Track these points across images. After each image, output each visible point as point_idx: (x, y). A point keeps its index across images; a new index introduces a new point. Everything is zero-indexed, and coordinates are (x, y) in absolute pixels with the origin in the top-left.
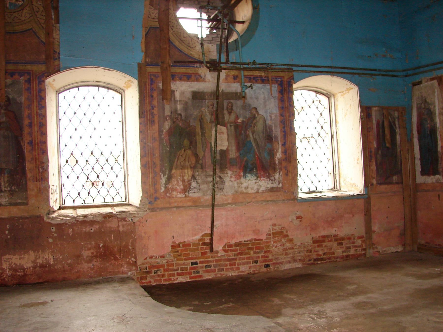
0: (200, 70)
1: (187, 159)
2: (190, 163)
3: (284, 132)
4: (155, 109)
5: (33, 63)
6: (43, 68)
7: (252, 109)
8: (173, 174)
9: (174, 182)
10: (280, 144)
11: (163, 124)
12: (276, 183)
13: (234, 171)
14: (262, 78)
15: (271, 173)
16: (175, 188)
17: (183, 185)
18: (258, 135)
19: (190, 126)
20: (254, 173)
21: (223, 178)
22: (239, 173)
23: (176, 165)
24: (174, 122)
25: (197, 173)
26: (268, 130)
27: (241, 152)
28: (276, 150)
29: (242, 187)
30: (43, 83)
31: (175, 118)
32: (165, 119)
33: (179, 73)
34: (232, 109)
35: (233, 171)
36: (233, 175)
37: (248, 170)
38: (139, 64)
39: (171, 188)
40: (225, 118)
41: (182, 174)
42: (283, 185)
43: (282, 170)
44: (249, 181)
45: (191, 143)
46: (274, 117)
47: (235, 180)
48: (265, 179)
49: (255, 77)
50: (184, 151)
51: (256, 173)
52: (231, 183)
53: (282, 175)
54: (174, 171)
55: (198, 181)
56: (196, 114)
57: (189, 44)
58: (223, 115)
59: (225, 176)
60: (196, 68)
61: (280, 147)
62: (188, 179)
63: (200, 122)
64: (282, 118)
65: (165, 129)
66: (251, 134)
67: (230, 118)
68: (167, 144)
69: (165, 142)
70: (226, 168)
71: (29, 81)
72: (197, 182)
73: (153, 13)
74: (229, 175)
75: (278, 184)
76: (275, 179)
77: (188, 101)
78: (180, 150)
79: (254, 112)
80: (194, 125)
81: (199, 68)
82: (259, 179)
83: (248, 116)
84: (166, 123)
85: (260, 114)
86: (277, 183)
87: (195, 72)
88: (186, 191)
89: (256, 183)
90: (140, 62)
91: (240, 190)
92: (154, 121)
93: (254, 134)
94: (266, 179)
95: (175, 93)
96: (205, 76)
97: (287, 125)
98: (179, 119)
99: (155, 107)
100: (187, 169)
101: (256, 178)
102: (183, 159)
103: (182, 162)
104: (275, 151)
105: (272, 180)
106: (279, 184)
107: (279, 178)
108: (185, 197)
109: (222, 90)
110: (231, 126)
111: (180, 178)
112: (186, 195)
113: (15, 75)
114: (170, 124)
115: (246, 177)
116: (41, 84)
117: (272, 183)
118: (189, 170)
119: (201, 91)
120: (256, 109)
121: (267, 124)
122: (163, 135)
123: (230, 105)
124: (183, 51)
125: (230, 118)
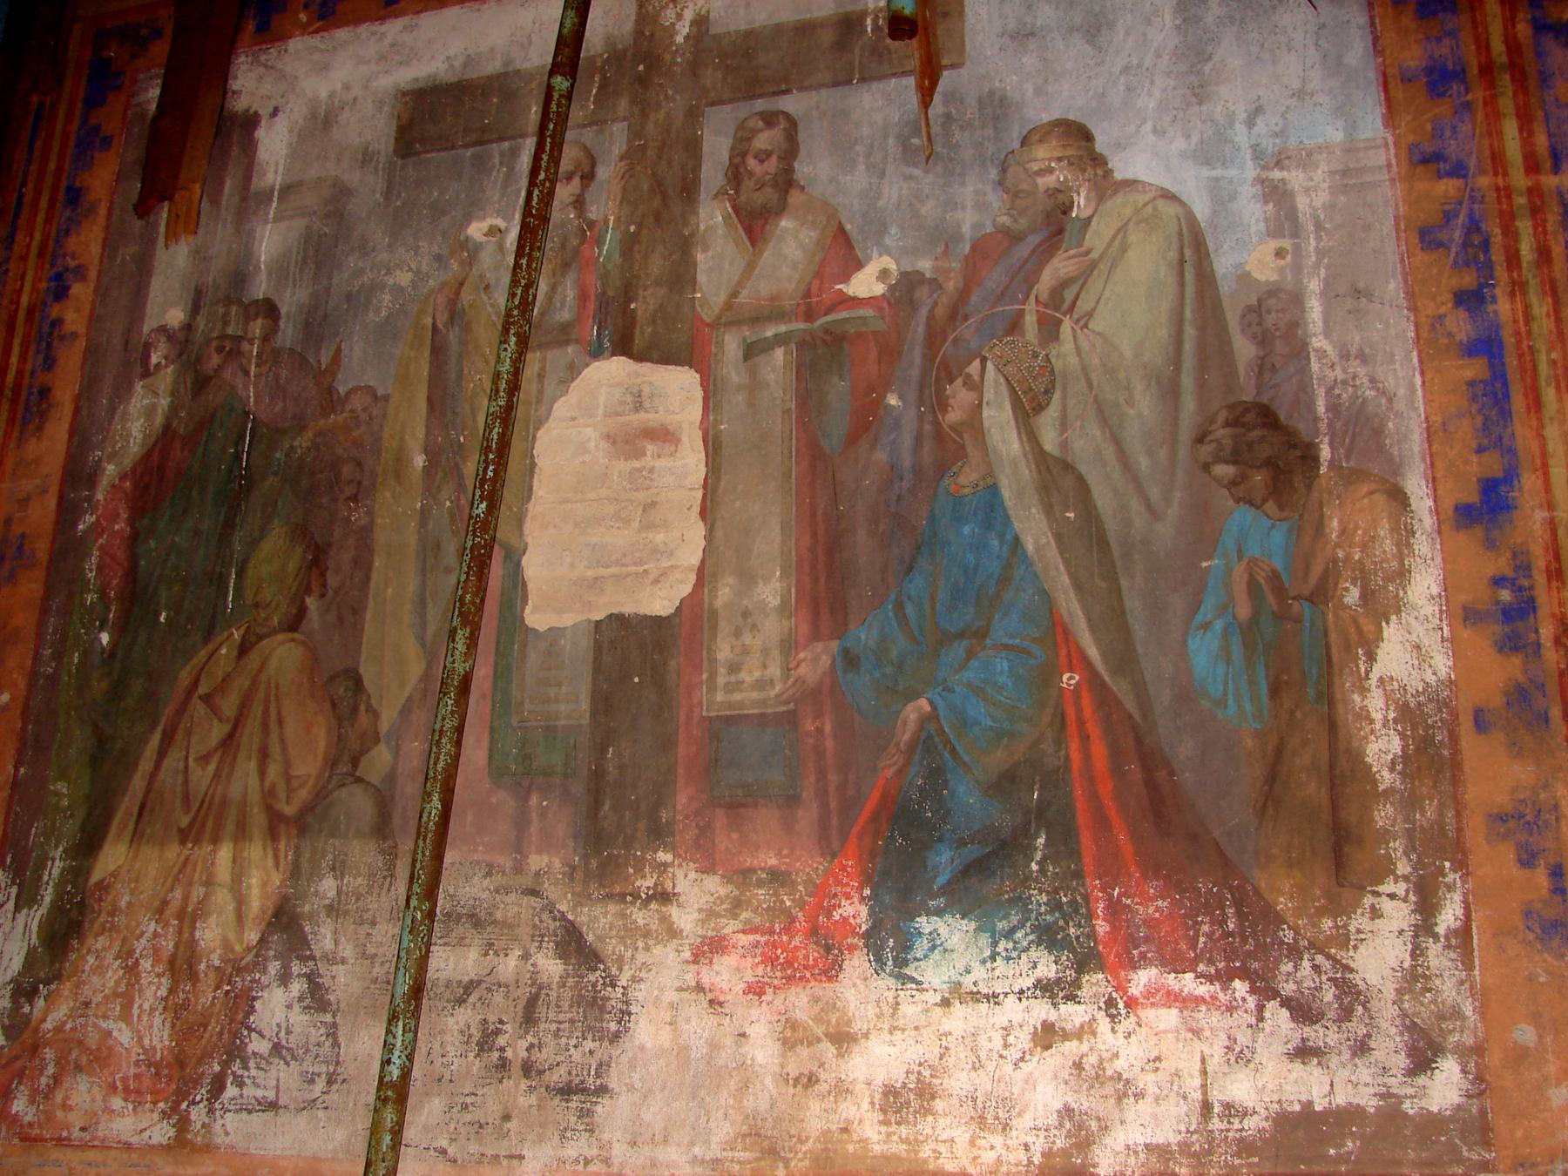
1: (250, 733)
2: (274, 771)
3: (1486, 346)
4: (77, 289)
7: (1025, 142)
8: (102, 887)
9: (99, 970)
10: (1416, 486)
11: (112, 410)
12: (1361, 1048)
13: (747, 872)
15: (1283, 904)
16: (93, 1040)
17: (176, 1009)
18: (1104, 421)
19: (330, 401)
20: (1020, 902)
21: (611, 947)
22: (822, 899)
23: (148, 791)
24: (201, 383)
25: (328, 886)
26: (1244, 350)
27: (863, 635)
28: (1367, 596)
29: (842, 1090)
31: (220, 349)
32: (137, 365)
34: (786, 182)
35: (742, 876)
36: (730, 927)
37: (944, 861)
39: (59, 1029)
40: (702, 278)
41: (178, 894)
42: (1480, 1083)
43: (1461, 865)
44: (946, 1003)
45: (317, 560)
46: (1321, 198)
47: (756, 990)
48: (1188, 983)
50: (243, 650)
51: (1056, 906)
52: (698, 1026)
53: (1463, 934)
54: (113, 857)
55: (322, 967)
56: (404, 278)
58: (684, 248)
59: (631, 932)
61: (1423, 545)
62: (227, 945)
63: (438, 351)
64: (1448, 187)
65: (112, 457)
66: (999, 419)
67: (750, 266)
68: (103, 594)
69: (91, 575)
70: (659, 834)
72: (312, 979)
74: (685, 919)
75: (1402, 1061)
76: (1351, 996)
77: (353, 178)
78: (207, 639)
79: (1050, 171)
80: (371, 391)
82: (1095, 983)
83: (968, 222)
84: (139, 399)
85: (1131, 184)
86: (1390, 1049)
88: (197, 1082)
89: (1047, 1036)
91: (816, 1118)
92: (45, 393)
93: (1039, 408)
94: (1203, 990)
95: (260, 133)
97: (1513, 260)
98: (245, 346)
99: (80, 273)
100: (242, 833)
101: (1047, 968)
102: (218, 732)
103: (205, 759)
104: (1352, 596)
105: (1302, 1011)
106: (1422, 1060)
107: (1414, 978)
108: (167, 1148)
109: (701, 22)
110: (751, 352)
111: (156, 935)
112: (183, 1124)
114: (164, 402)
115: (905, 946)
117: (1304, 1052)
118: (255, 851)
119: (493, 67)
120: (1077, 134)
121: (1225, 287)
122: (93, 510)
123: (763, 140)
125: (750, 266)
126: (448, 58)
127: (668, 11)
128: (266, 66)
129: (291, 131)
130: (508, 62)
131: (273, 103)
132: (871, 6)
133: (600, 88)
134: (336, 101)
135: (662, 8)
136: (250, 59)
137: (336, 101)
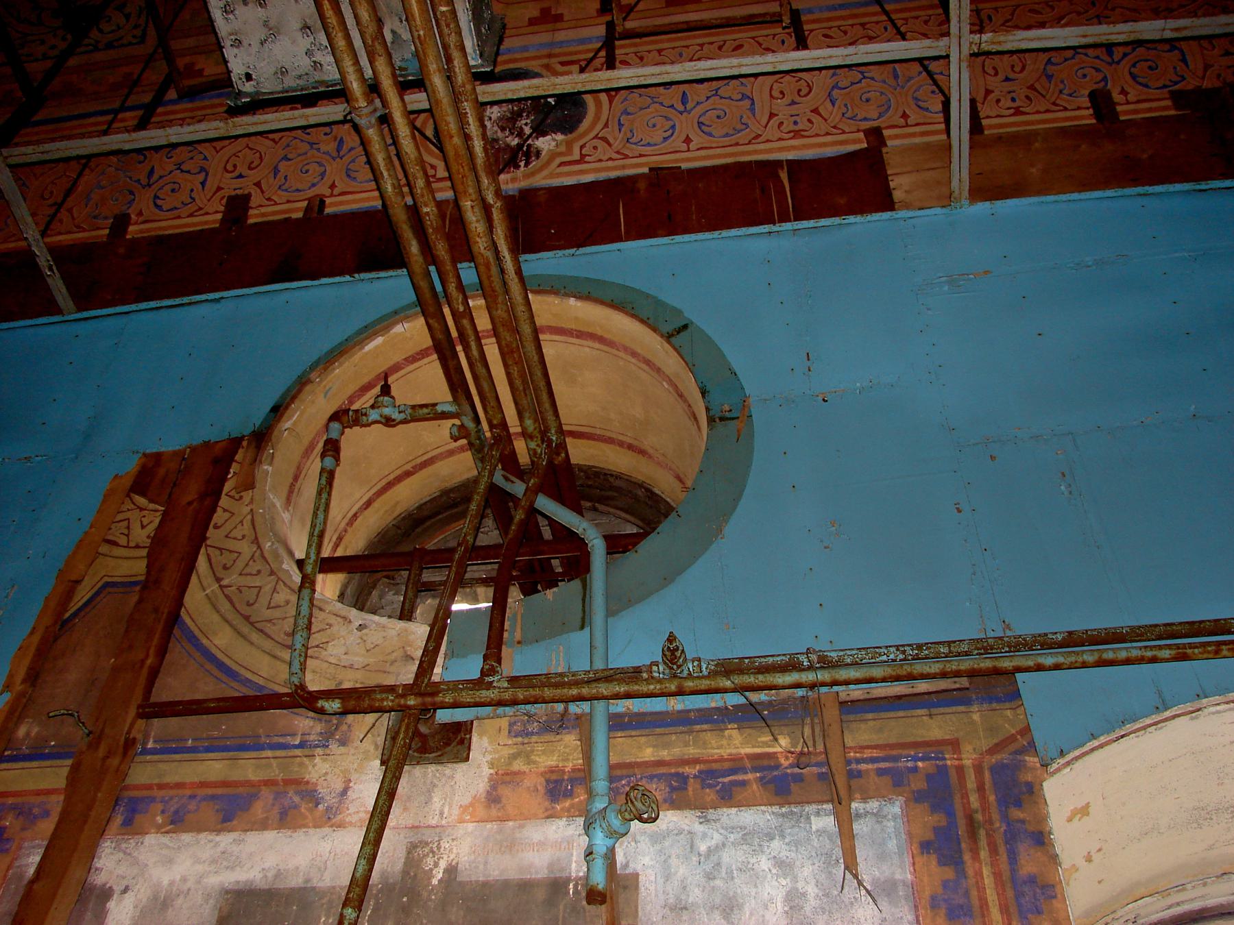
0: (317, 760)
14: (777, 767)
33: (179, 786)
49: (715, 766)
60: (298, 752)
73: (143, 527)
81: (319, 751)
95: (111, 905)
96: (344, 792)
109: (451, 870)
119: (296, 882)
124: (242, 672)
126: (263, 869)
127: (429, 859)
128: (125, 853)
129: (136, 907)
130: (307, 881)
131: (125, 883)
132: (574, 875)
133: (373, 911)
134: (175, 889)
135: (424, 856)
136: (114, 845)
137: (175, 889)
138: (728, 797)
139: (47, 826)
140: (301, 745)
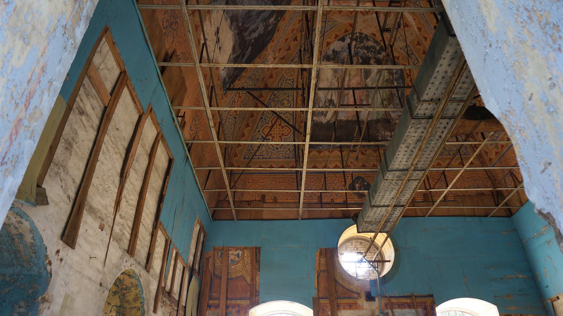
5: (241, 299)
6: (248, 302)
30: (247, 313)
33: (343, 303)
38: (313, 298)
57: (349, 281)
71: (238, 312)
87: (354, 302)
90: (314, 296)
113: (229, 307)
116: (246, 314)
138: (404, 308)
139: (329, 308)
140: (356, 298)
